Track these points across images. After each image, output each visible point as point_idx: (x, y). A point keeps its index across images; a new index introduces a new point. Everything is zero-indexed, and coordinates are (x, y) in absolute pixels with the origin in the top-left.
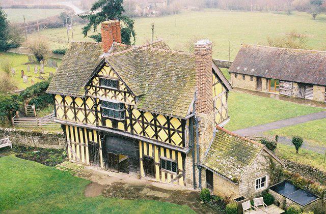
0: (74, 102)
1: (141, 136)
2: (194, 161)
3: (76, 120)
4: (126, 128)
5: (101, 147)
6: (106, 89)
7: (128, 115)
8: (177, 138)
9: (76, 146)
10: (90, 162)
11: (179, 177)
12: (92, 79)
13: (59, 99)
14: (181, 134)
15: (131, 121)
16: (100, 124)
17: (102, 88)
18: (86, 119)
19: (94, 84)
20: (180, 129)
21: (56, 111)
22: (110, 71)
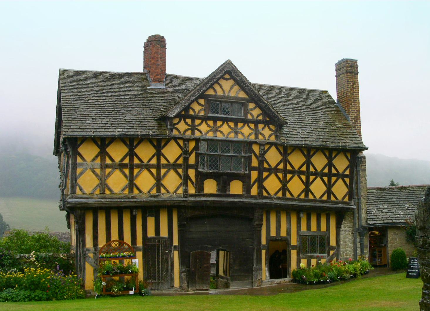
0: (132, 154)
1: (279, 198)
2: (354, 224)
3: (131, 191)
4: (247, 188)
5: (176, 243)
6: (215, 120)
7: (255, 163)
12: (193, 101)
14: (347, 180)
15: (260, 174)
16: (192, 190)
17: (210, 118)
18: (159, 185)
20: (347, 172)
21: (75, 179)
22: (232, 87)
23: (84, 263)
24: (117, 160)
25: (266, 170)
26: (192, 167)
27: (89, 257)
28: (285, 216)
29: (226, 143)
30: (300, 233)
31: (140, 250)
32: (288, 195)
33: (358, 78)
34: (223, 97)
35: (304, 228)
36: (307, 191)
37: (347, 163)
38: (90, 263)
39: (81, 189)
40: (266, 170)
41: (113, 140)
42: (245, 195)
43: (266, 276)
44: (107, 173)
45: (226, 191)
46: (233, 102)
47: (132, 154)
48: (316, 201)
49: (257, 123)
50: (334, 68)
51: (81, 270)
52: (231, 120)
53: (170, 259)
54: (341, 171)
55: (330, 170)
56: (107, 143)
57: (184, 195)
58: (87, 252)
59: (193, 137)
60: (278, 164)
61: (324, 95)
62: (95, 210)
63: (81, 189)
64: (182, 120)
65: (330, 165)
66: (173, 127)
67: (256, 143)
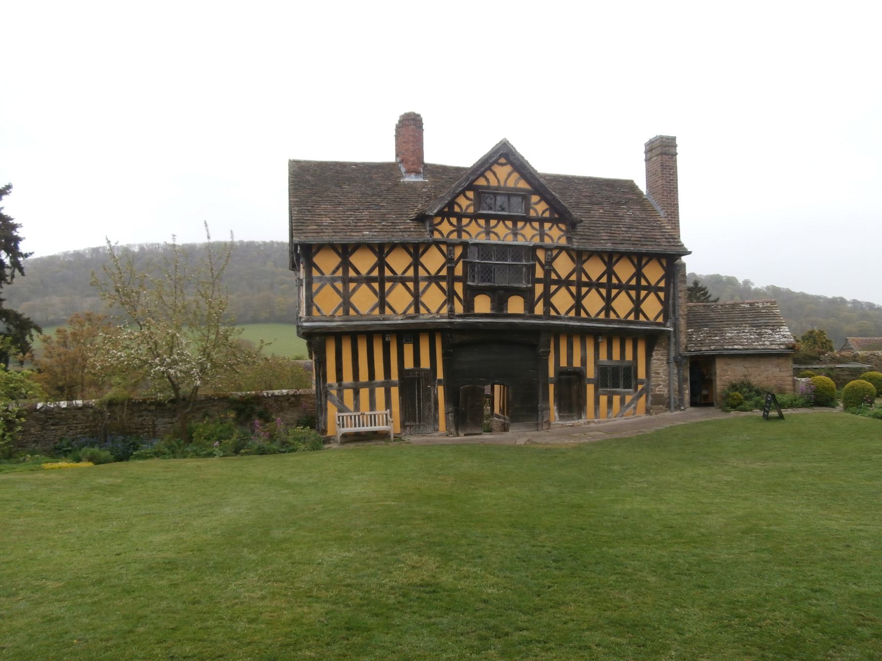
0: (381, 264)
1: (571, 319)
3: (382, 311)
4: (530, 305)
5: (440, 375)
6: (488, 218)
7: (539, 273)
8: (652, 307)
9: (356, 393)
10: (403, 426)
11: (640, 396)
12: (458, 195)
13: (327, 262)
14: (662, 295)
16: (459, 308)
18: (417, 302)
19: (457, 209)
20: (662, 284)
22: (509, 175)
23: (326, 402)
24: (364, 271)
25: (554, 282)
26: (458, 279)
27: (332, 395)
28: (579, 340)
29: (503, 250)
30: (598, 364)
31: (395, 385)
32: (583, 315)
33: (676, 161)
34: (497, 188)
35: (603, 356)
36: (608, 308)
37: (662, 273)
38: (333, 402)
39: (319, 310)
40: (554, 282)
41: (357, 246)
42: (528, 315)
43: (555, 417)
44: (350, 290)
45: (502, 310)
46: (510, 194)
47: (381, 264)
48: (619, 321)
49: (542, 221)
50: (643, 149)
51: (322, 411)
52: (509, 218)
53: (432, 396)
54: (653, 283)
55: (638, 281)
56: (349, 250)
57: (449, 315)
58: (328, 389)
59: (459, 241)
60: (570, 275)
61: (629, 186)
62: (338, 335)
63: (319, 310)
64: (446, 220)
65: (639, 275)
66: (433, 229)
67: (541, 247)
